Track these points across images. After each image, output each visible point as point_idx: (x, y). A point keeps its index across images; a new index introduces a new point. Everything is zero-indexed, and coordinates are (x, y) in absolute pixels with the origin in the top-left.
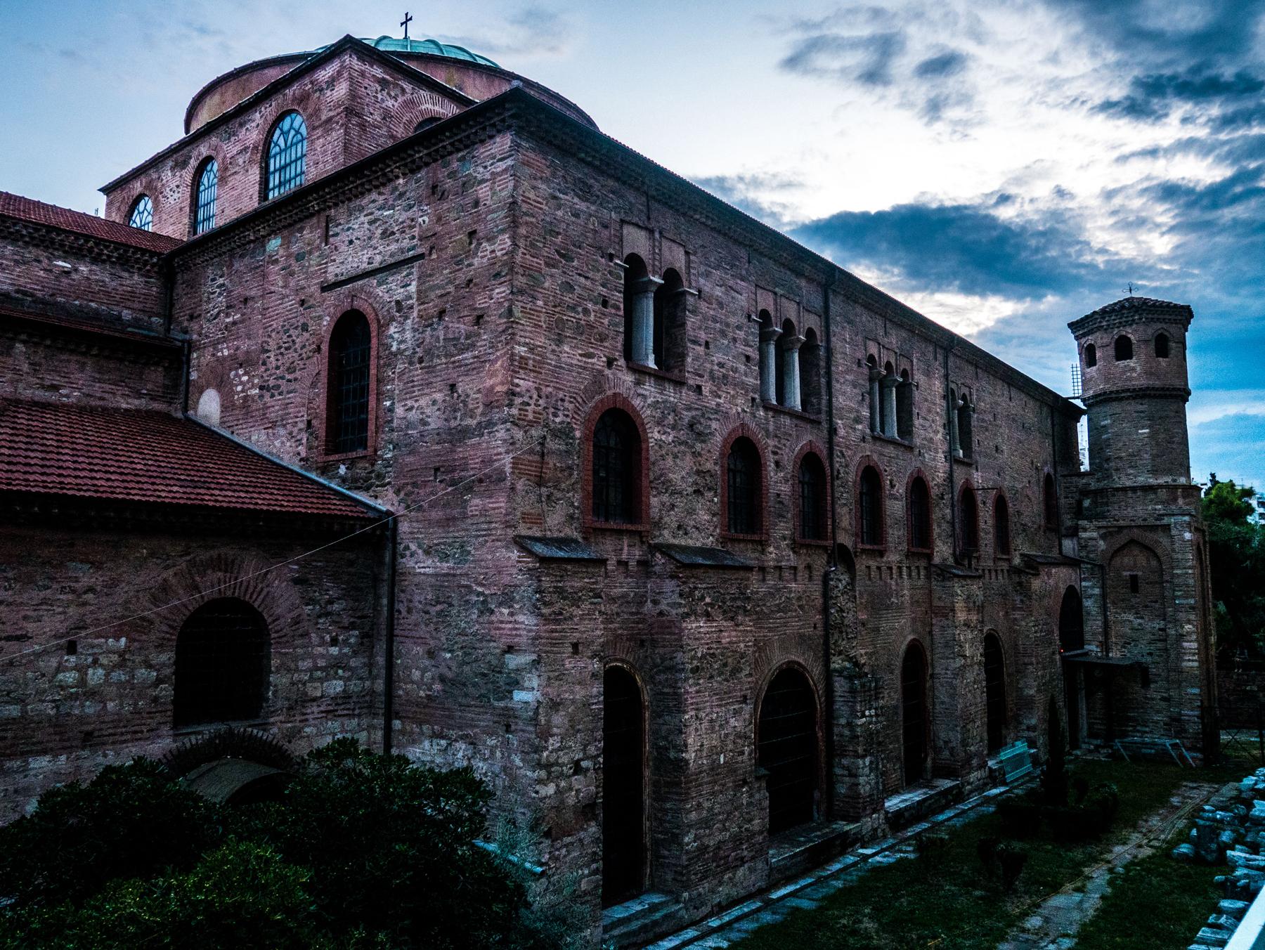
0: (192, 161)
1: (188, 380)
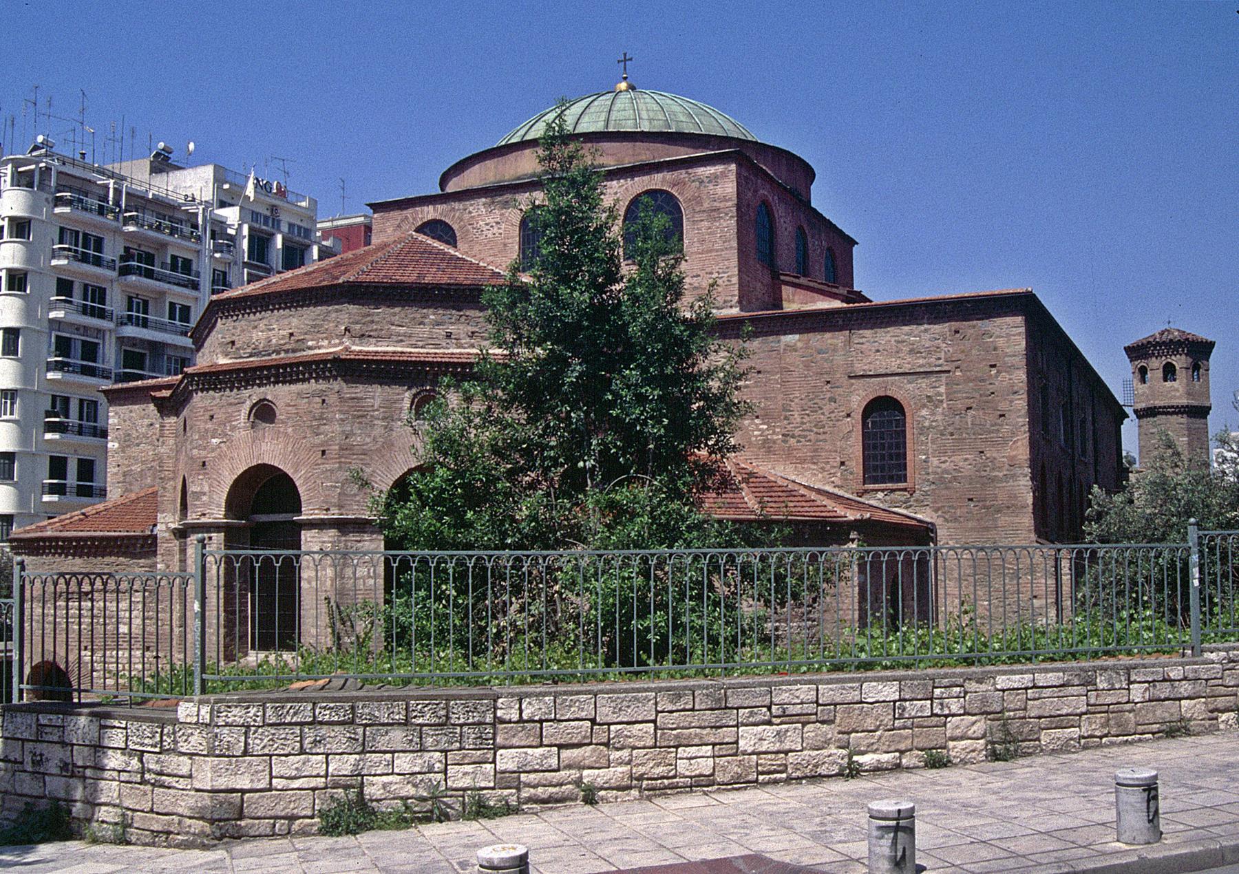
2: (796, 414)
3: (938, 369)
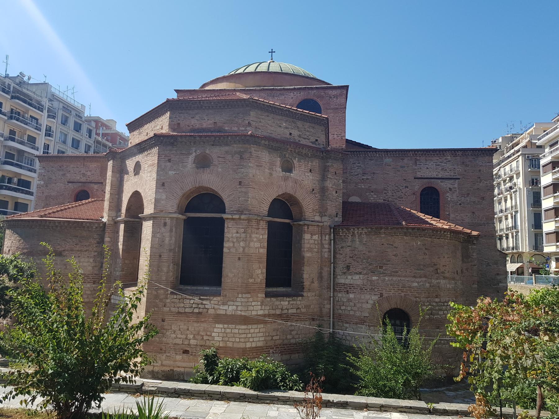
2: (390, 192)
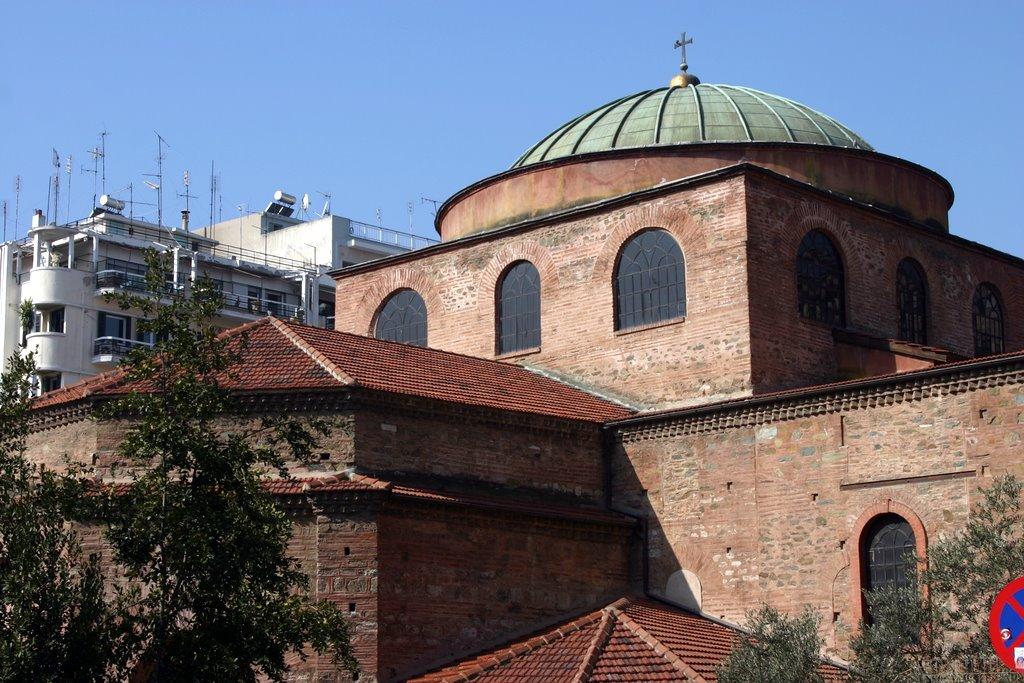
0: (493, 261)
1: (646, 559)
2: (776, 544)
3: (958, 469)
